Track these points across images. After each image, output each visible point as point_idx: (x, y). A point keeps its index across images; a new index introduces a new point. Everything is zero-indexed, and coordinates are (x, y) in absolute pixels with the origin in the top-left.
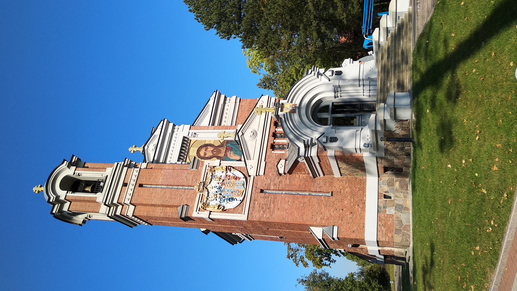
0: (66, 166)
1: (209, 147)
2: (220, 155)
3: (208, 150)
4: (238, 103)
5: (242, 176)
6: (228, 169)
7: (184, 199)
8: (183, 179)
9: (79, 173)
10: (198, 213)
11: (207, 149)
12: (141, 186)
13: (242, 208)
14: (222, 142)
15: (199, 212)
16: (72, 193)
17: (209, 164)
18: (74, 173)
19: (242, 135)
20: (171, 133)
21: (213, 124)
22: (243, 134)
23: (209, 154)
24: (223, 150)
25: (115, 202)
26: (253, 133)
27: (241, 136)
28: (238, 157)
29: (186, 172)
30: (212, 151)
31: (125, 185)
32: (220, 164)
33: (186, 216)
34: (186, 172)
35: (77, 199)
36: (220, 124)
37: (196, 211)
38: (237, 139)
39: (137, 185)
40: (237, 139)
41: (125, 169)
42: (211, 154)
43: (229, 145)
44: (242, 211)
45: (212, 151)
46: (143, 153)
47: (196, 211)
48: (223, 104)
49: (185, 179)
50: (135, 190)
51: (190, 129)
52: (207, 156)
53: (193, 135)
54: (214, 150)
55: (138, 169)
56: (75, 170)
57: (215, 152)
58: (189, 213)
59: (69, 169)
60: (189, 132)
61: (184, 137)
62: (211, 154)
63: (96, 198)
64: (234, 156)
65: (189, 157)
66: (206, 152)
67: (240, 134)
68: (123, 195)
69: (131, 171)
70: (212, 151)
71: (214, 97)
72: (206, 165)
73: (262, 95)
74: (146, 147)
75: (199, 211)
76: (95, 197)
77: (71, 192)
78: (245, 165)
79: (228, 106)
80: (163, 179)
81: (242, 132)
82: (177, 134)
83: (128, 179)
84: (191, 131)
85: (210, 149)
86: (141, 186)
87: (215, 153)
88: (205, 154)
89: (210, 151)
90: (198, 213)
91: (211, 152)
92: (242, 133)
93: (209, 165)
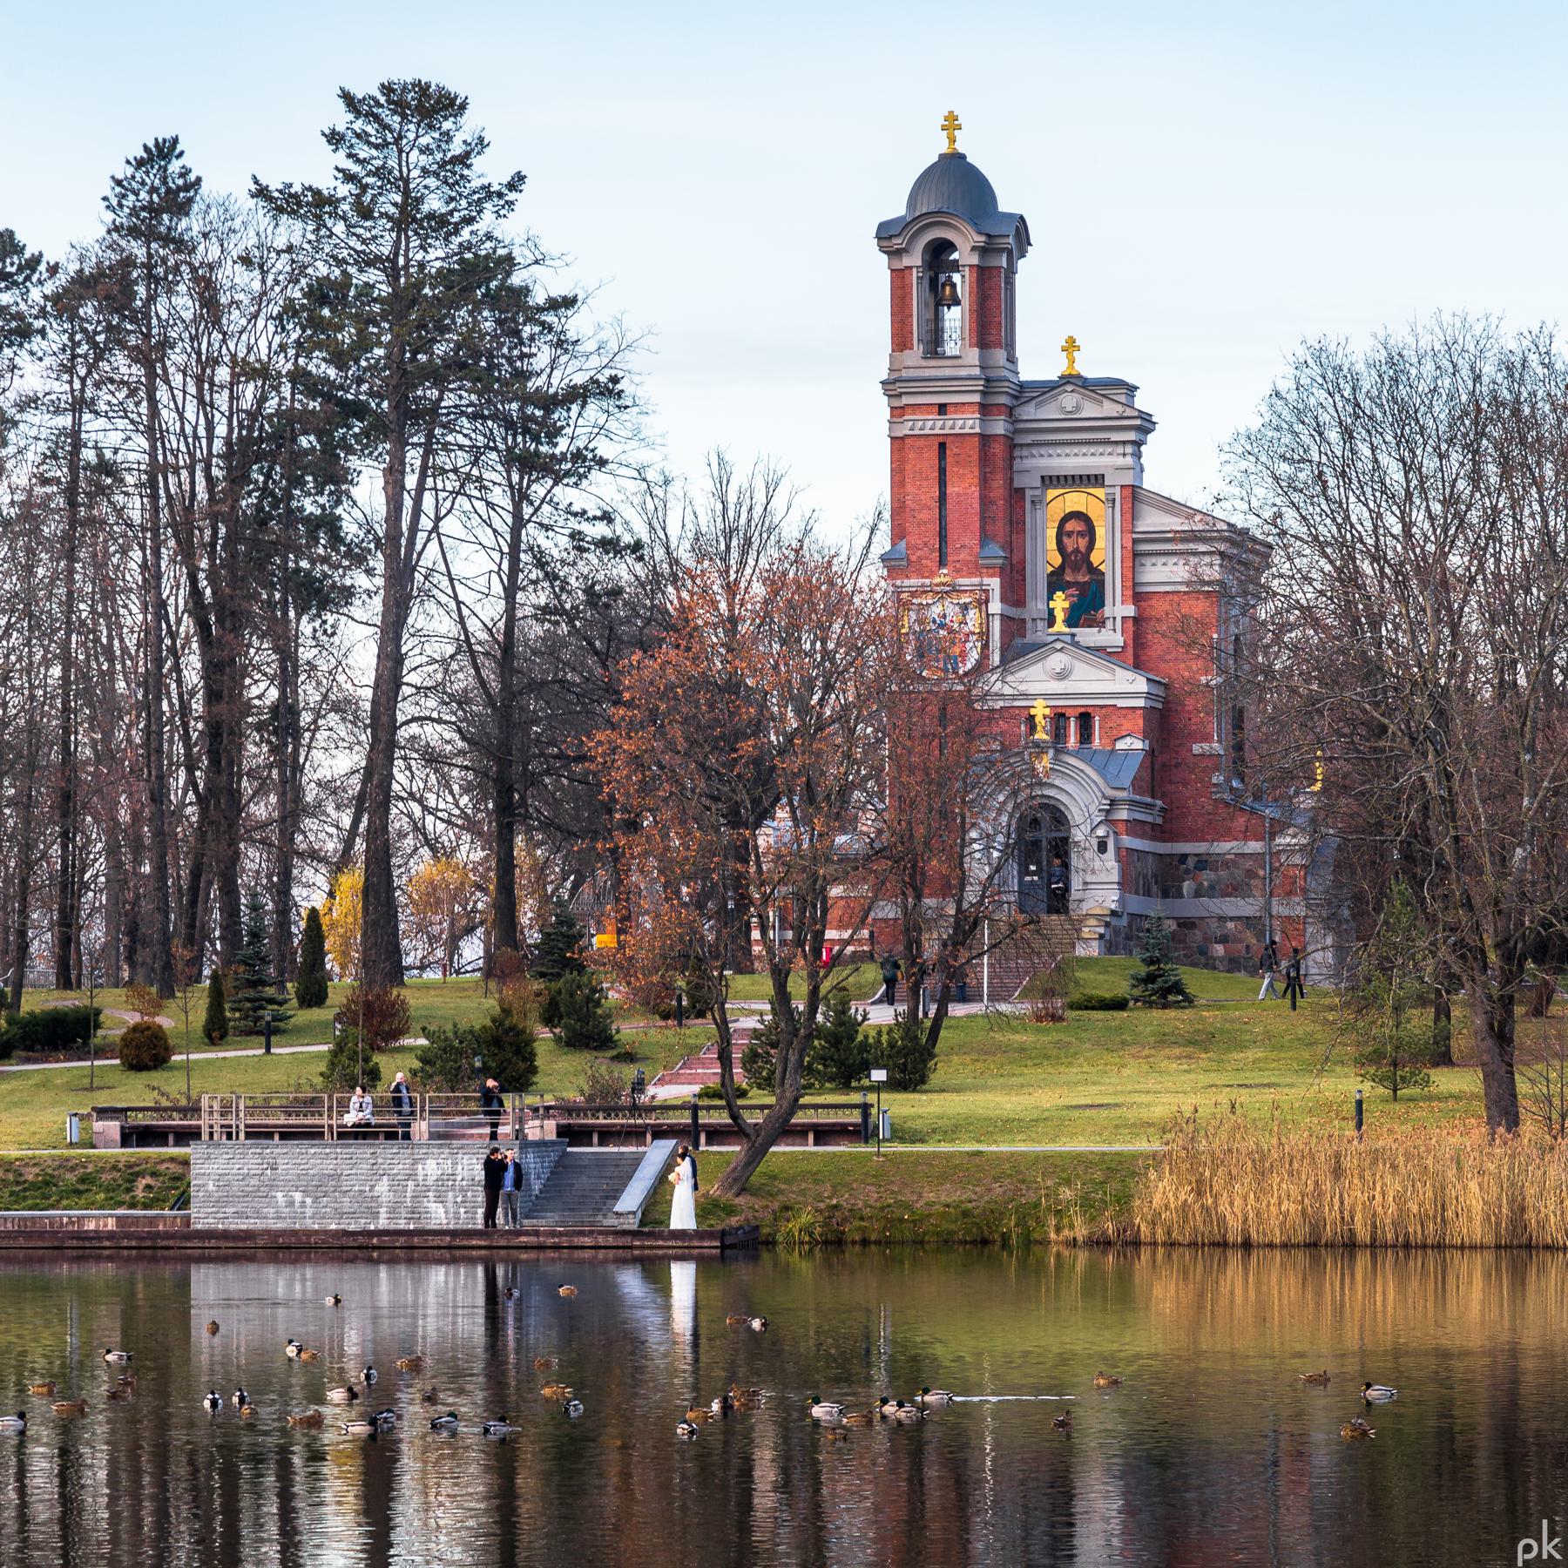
2: (1068, 571)
5: (969, 666)
6: (985, 636)
7: (919, 553)
12: (942, 446)
22: (1060, 650)
23: (1070, 544)
24: (1083, 578)
31: (942, 409)
39: (941, 440)
42: (1070, 549)
43: (1093, 587)
45: (1077, 550)
52: (1065, 539)
62: (1070, 549)
67: (1058, 645)
70: (1077, 550)
74: (1069, 388)
80: (958, 495)
85: (1083, 543)
86: (942, 446)
88: (1070, 534)
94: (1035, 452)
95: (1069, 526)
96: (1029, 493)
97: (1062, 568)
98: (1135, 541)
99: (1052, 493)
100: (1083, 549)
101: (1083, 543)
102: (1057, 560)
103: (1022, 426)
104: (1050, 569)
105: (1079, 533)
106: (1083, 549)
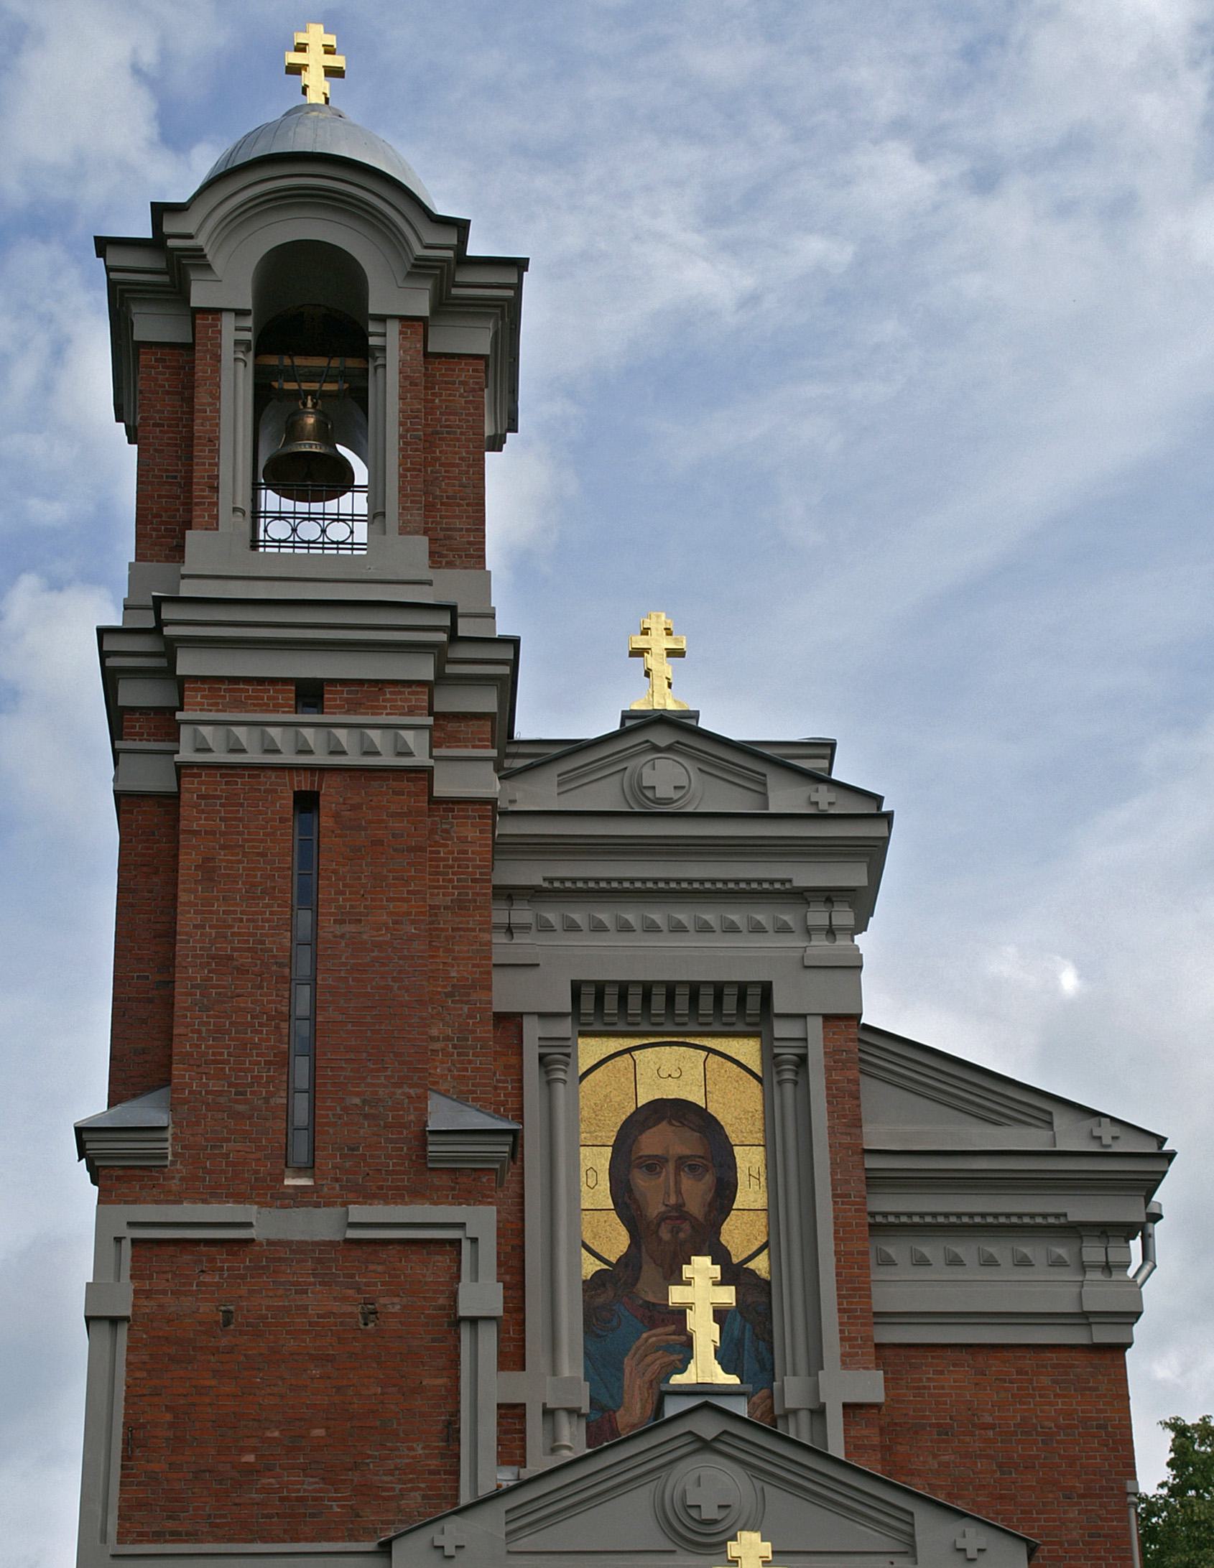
0: (420, 251)
1: (709, 1179)
3: (687, 1182)
4: (1076, 1336)
8: (358, 1085)
9: (383, 349)
10: (118, 1240)
11: (693, 1168)
12: (307, 802)
13: (158, 1537)
14: (752, 1272)
15: (126, 1245)
16: (237, 343)
17: (474, 1240)
18: (382, 319)
19: (699, 1439)
20: (788, 886)
21: (875, 1181)
22: (705, 1446)
25: (188, 664)
26: (714, 1522)
27: (690, 1433)
28: (643, 1408)
29: (412, 1092)
30: (679, 1206)
32: (474, 1321)
33: (97, 1163)
34: (412, 1092)
35: (202, 397)
36: (881, 1228)
37: (131, 1225)
38: (672, 1407)
40: (672, 1407)
41: (424, 669)
42: (655, 1209)
44: (143, 1537)
45: (678, 1213)
46: (629, 723)
47: (131, 1225)
48: (1062, 1220)
49: (358, 1094)
50: (273, 775)
51: (827, 1018)
52: (641, 1181)
53: (788, 1052)
54: (686, 1226)
55: (421, 758)
56: (402, 318)
57: (675, 1231)
58: (118, 1178)
59: (410, 275)
60: (804, 1016)
61: (766, 990)
62: (655, 1209)
63: (213, 523)
64: (648, 1376)
65: (629, 1051)
66: (671, 1166)
67: (708, 1427)
68: (238, 705)
69: (411, 712)
70: (678, 1213)
71: (1117, 1148)
72: (461, 1226)
73: (1032, 1551)
75: (135, 1242)
76: (217, 517)
77: (248, 336)
78: (465, 1499)
79: (1058, 1263)
81: (725, 1432)
82: (784, 929)
83: (353, 707)
84: (815, 1029)
86: (307, 802)
87: (665, 1235)
88: (653, 1165)
89: (679, 1192)
90: (118, 1240)
91: (673, 1200)
92: (716, 1439)
93: (466, 1246)
94: (552, 916)
95: (653, 1142)
96: (533, 1031)
97: (629, 1262)
98: (875, 1181)
99: (590, 1050)
100: (695, 1207)
101: (695, 1193)
102: (615, 1241)
103: (507, 828)
104: (590, 1266)
105: (681, 1162)
106: (695, 1207)
